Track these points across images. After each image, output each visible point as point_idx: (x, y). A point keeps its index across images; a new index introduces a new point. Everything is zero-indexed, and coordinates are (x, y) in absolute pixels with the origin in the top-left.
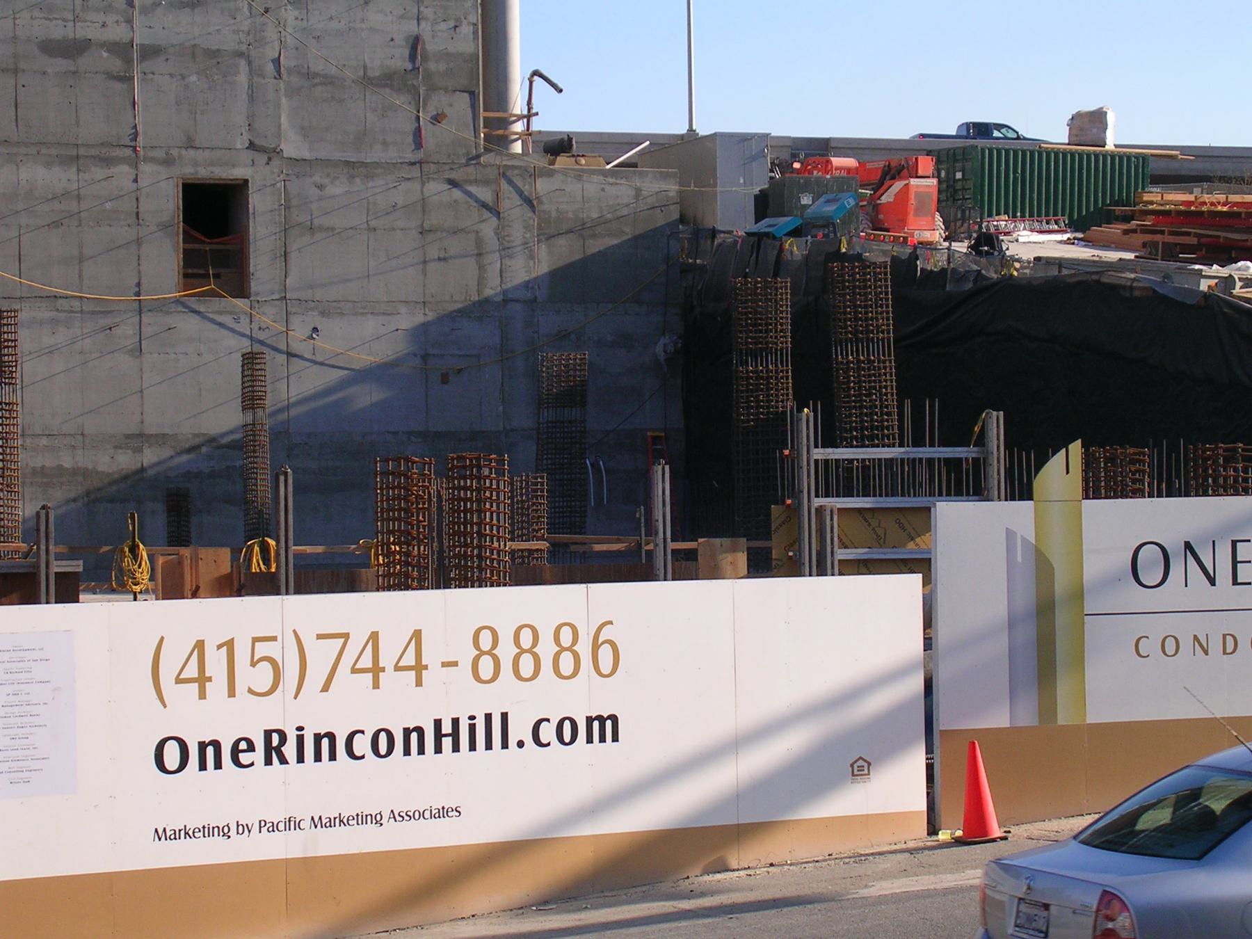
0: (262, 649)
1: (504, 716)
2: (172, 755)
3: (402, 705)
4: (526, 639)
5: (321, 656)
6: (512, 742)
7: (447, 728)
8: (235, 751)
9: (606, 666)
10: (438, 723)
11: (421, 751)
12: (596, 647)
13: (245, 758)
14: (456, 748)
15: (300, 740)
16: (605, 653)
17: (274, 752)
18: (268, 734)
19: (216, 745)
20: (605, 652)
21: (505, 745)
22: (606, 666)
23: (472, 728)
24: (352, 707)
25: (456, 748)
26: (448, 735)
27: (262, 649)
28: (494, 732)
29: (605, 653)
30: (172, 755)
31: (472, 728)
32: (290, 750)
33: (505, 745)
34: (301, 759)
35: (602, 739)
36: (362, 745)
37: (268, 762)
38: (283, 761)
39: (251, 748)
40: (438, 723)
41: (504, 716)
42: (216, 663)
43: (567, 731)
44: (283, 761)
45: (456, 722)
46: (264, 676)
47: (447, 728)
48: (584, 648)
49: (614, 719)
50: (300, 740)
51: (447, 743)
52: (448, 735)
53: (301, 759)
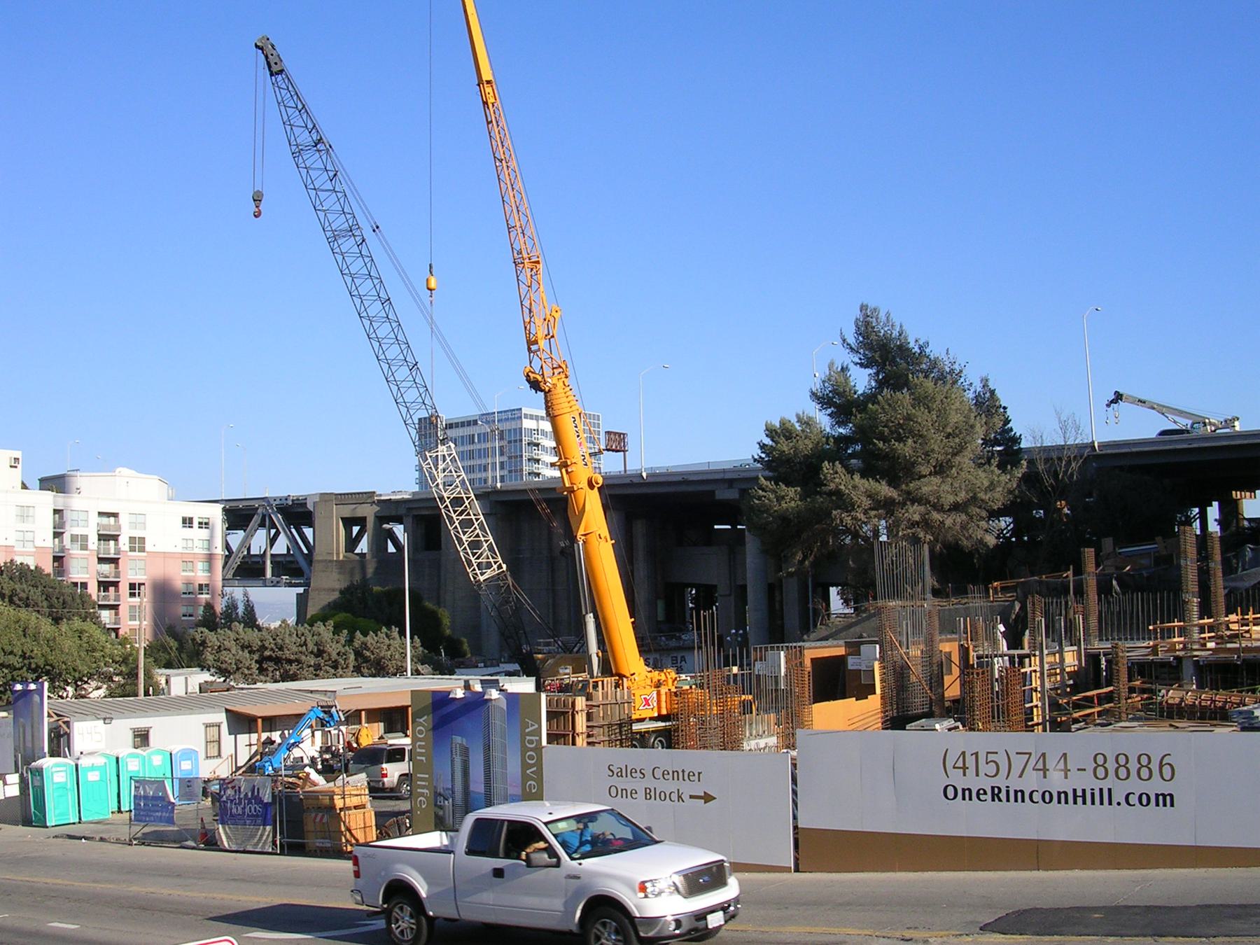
0: (991, 757)
1: (1110, 790)
2: (950, 792)
3: (1056, 782)
4: (1122, 760)
5: (1018, 762)
6: (1114, 803)
7: (1079, 793)
8: (978, 794)
9: (1167, 776)
10: (1075, 791)
11: (1066, 802)
12: (1161, 766)
13: (982, 797)
14: (1084, 803)
15: (1008, 792)
16: (1167, 771)
17: (995, 795)
18: (993, 788)
19: (970, 790)
20: (1166, 767)
21: (1110, 803)
22: (1167, 776)
23: (1093, 794)
24: (1031, 782)
25: (1084, 803)
26: (1080, 797)
27: (991, 757)
28: (1105, 797)
29: (1167, 771)
30: (950, 792)
31: (1093, 794)
32: (1003, 796)
33: (1110, 803)
34: (1008, 800)
35: (1165, 805)
36: (1036, 797)
37: (993, 800)
38: (1000, 800)
39: (985, 793)
40: (1075, 791)
41: (1110, 790)
42: (970, 761)
43: (1144, 800)
44: (1000, 800)
45: (1084, 791)
46: (991, 769)
47: (1079, 793)
48: (1155, 766)
49: (1171, 796)
50: (1008, 792)
51: (1080, 800)
52: (1080, 797)
53: (1008, 800)
